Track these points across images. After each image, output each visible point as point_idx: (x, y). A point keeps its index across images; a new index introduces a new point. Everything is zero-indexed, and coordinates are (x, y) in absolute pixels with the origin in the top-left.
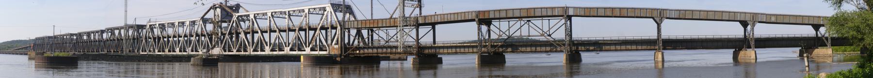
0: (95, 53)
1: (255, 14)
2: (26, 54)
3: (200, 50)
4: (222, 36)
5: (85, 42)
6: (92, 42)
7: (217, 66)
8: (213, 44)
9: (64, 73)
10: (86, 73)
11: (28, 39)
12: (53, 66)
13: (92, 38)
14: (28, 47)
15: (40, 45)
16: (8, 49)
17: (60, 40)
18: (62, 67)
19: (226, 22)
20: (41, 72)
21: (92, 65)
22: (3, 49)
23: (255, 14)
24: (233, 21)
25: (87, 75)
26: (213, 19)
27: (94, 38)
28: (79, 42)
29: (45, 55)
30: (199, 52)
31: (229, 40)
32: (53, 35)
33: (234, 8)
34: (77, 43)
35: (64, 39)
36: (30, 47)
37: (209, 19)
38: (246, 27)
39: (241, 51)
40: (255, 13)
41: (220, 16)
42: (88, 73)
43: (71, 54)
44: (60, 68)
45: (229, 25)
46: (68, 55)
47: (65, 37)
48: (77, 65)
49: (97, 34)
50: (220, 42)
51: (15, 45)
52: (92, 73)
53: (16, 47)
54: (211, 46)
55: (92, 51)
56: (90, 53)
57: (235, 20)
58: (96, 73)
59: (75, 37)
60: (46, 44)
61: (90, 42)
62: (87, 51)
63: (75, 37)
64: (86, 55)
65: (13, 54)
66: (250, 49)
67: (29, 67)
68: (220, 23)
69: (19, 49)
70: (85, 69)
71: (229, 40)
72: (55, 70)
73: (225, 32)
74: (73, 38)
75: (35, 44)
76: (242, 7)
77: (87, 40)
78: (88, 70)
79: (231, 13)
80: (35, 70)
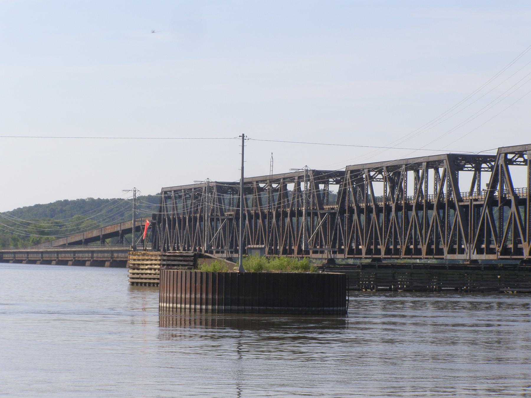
0: (424, 259)
2: (121, 264)
5: (379, 210)
6: (409, 207)
9: (289, 346)
10: (381, 348)
11: (129, 196)
12: (235, 317)
13: (410, 192)
14: (129, 231)
15: (182, 222)
16: (37, 243)
17: (271, 200)
18: (275, 319)
20: (187, 342)
21: (409, 312)
22: (15, 240)
25: (385, 359)
27: (419, 192)
28: (351, 211)
29: (205, 267)
32: (236, 178)
34: (342, 211)
35: (286, 194)
36: (138, 229)
42: (388, 347)
43: (319, 263)
44: (268, 326)
46: (306, 268)
47: (291, 187)
48: (345, 313)
49: (431, 172)
51: (70, 225)
52: (410, 349)
53: (78, 230)
55: (408, 251)
56: (403, 260)
58: (428, 349)
59: (334, 188)
60: (207, 215)
61: (399, 208)
62: (388, 251)
63: (334, 188)
64: (387, 267)
65: (64, 263)
67: (133, 323)
69: (88, 241)
70: (378, 332)
72: (247, 332)
74: (326, 193)
75: (158, 220)
77: (387, 199)
78: (390, 336)
80: (159, 337)
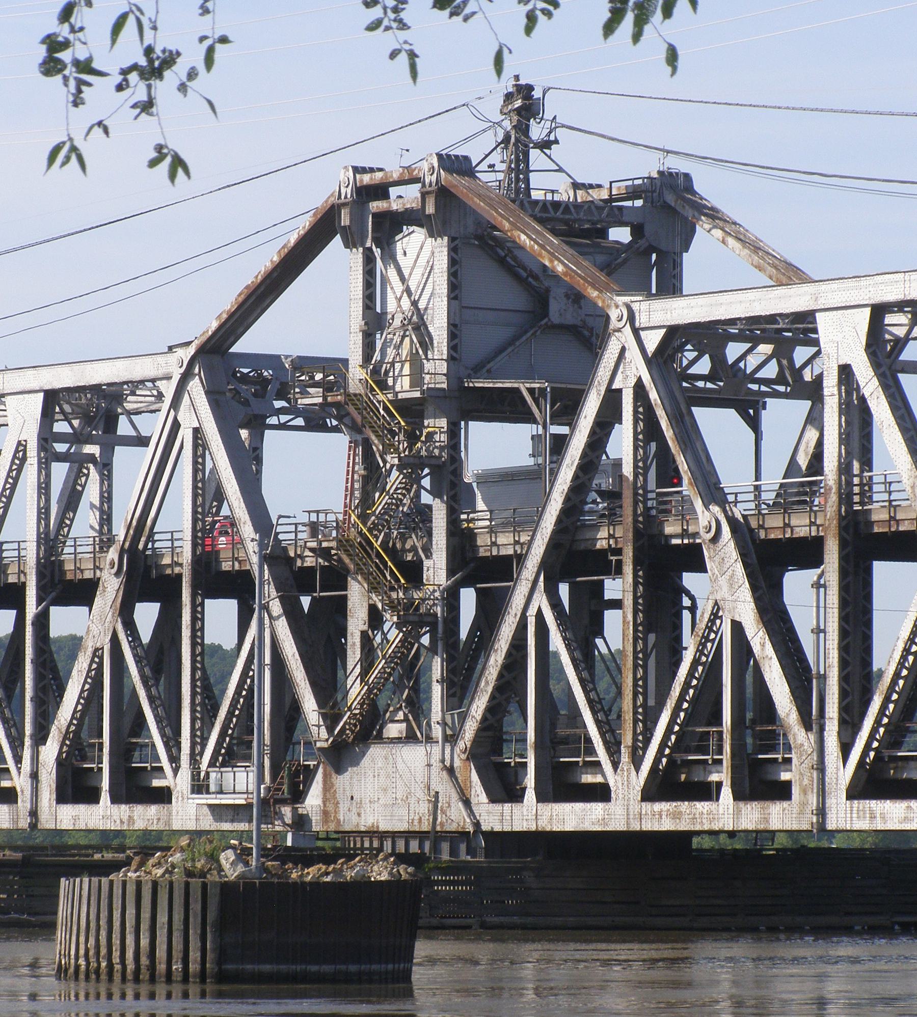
1: (879, 311)
3: (181, 783)
4: (468, 598)
7: (406, 977)
8: (355, 690)
19: (526, 417)
23: (879, 311)
24: (612, 398)
26: (357, 374)
30: (163, 796)
31: (557, 642)
33: (621, 235)
37: (303, 364)
38: (773, 478)
39: (708, 792)
40: (890, 291)
41: (438, 327)
45: (560, 444)
50: (437, 667)
54: (331, 718)
57: (625, 384)
66: (821, 767)
68: (437, 425)
71: (557, 642)
73: (505, 543)
76: (714, 215)
79: (577, 298)
